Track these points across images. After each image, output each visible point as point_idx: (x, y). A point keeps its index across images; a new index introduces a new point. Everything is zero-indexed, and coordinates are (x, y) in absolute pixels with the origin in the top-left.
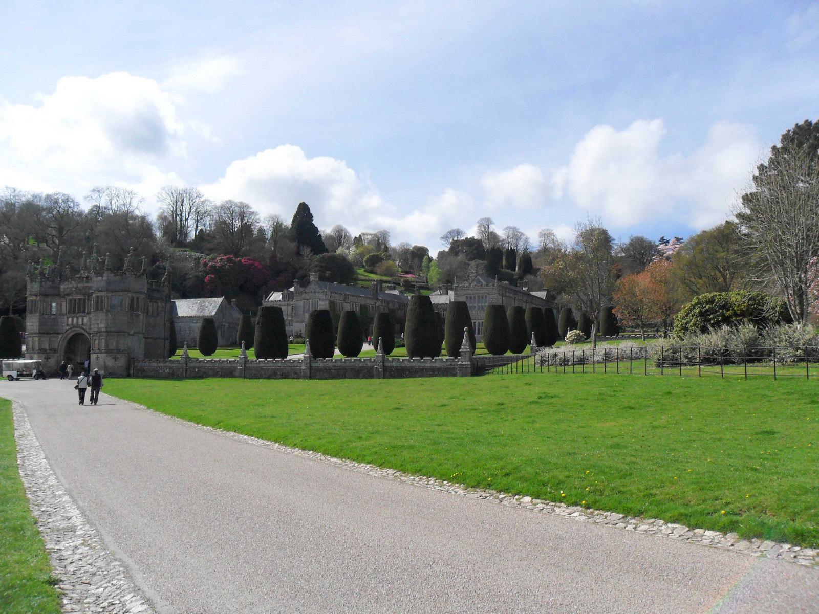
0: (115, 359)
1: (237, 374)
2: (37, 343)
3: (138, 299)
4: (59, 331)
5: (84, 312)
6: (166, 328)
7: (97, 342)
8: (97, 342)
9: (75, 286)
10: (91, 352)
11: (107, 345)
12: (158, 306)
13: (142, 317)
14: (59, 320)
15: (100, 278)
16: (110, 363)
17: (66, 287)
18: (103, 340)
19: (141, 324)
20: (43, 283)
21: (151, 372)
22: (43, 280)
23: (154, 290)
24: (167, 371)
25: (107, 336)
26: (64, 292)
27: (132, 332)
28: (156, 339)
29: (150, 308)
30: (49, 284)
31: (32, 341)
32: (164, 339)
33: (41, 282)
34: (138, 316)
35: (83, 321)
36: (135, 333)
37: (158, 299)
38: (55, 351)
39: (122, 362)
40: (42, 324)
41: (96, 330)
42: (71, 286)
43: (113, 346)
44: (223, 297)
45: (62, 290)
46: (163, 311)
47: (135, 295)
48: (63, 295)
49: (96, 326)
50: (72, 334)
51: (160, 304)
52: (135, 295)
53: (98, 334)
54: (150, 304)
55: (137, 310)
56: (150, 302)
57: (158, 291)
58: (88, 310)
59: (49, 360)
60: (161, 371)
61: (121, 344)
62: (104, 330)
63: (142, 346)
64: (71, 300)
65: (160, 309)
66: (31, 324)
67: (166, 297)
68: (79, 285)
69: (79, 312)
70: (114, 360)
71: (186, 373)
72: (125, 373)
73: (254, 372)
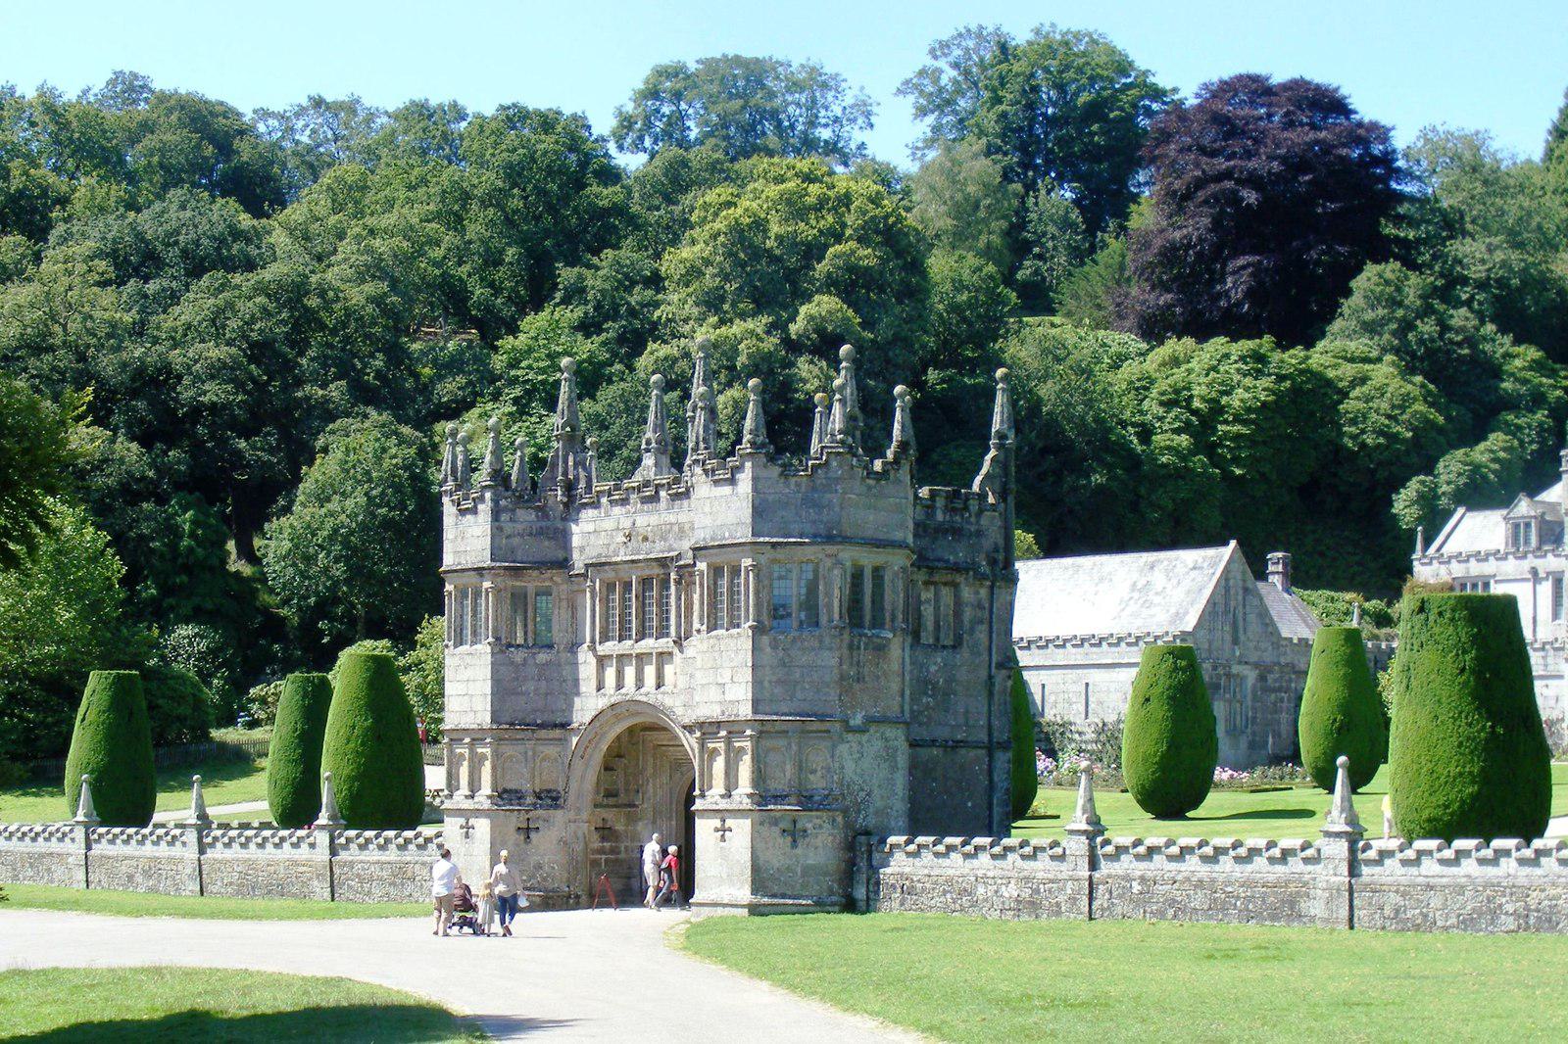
0: (795, 834)
1: (1316, 908)
2: (488, 765)
3: (877, 571)
6: (996, 698)
9: (626, 523)
10: (698, 805)
11: (759, 777)
12: (958, 603)
15: (727, 490)
16: (779, 853)
17: (590, 527)
18: (747, 759)
19: (895, 687)
20: (504, 517)
21: (945, 893)
22: (503, 503)
23: (941, 530)
24: (1011, 891)
25: (757, 739)
26: (582, 549)
27: (857, 720)
28: (958, 744)
29: (928, 612)
30: (527, 516)
31: (471, 760)
32: (991, 748)
33: (496, 514)
34: (881, 648)
36: (871, 720)
37: (957, 568)
38: (551, 798)
39: (822, 846)
40: (502, 690)
42: (609, 524)
43: (783, 777)
44: (1233, 543)
45: (576, 541)
46: (981, 622)
47: (868, 559)
49: (714, 694)
50: (619, 728)
51: (967, 593)
52: (868, 559)
54: (927, 595)
55: (878, 623)
56: (927, 583)
57: (957, 532)
58: (679, 626)
59: (533, 835)
61: (814, 772)
62: (745, 711)
63: (901, 780)
65: (968, 614)
66: (461, 688)
67: (993, 562)
68: (641, 521)
69: (642, 635)
70: (790, 838)
71: (1091, 899)
72: (834, 898)
73: (1395, 899)
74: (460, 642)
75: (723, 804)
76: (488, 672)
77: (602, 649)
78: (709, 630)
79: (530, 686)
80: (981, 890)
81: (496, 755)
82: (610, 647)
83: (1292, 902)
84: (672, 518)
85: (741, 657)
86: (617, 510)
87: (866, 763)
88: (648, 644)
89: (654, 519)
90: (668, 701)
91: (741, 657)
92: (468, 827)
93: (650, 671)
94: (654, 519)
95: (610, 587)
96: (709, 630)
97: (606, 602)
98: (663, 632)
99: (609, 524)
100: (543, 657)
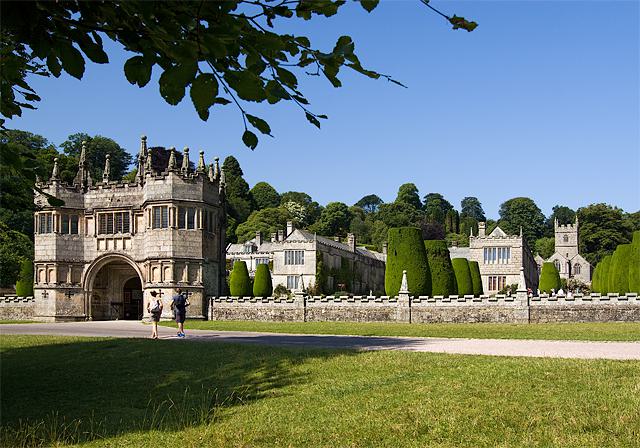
4: (86, 259)
5: (126, 230)
7: (157, 272)
8: (157, 272)
13: (216, 239)
14: (85, 244)
26: (91, 204)
35: (124, 245)
41: (157, 255)
42: (103, 196)
45: (87, 201)
48: (89, 209)
49: (156, 249)
52: (209, 209)
53: (160, 261)
60: (259, 313)
62: (170, 254)
64: (102, 216)
73: (428, 314)
74: (41, 232)
75: (160, 285)
76: (55, 242)
77: (99, 237)
78: (153, 228)
79: (70, 248)
80: (259, 313)
81: (57, 270)
82: (102, 236)
83: (387, 316)
84: (130, 194)
85: (168, 237)
86: (106, 191)
87: (209, 274)
88: (120, 234)
89: (122, 194)
90: (128, 253)
91: (168, 237)
92: (45, 295)
93: (120, 243)
94: (122, 194)
95: (102, 216)
96: (153, 228)
97: (100, 221)
98: (126, 230)
99: (103, 196)
100: (75, 238)
